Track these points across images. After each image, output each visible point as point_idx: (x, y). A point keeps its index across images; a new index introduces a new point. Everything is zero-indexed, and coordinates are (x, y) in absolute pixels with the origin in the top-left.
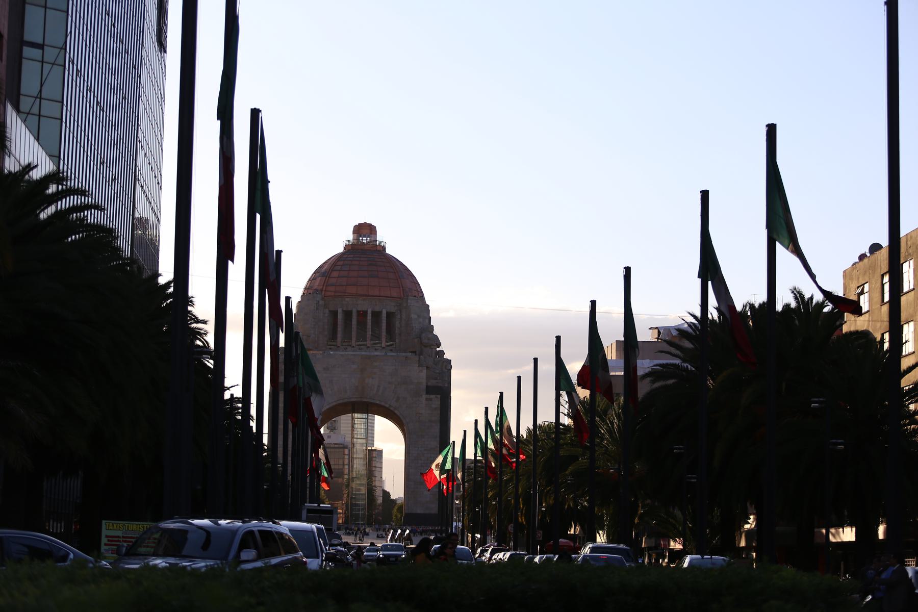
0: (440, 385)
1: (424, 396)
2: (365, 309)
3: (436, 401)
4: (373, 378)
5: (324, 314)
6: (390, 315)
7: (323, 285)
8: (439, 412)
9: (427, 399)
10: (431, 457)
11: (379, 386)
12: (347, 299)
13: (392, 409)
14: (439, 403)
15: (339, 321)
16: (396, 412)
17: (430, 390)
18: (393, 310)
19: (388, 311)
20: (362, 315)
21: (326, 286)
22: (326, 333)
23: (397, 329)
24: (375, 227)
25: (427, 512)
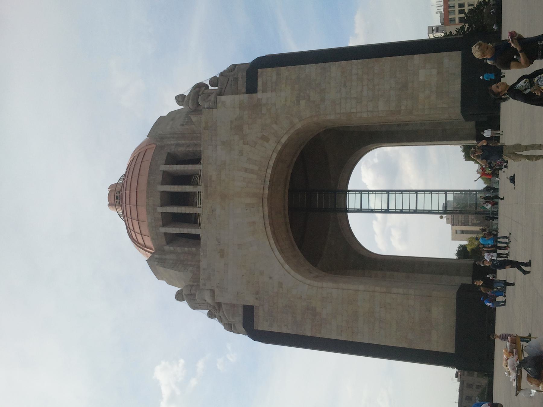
0: (245, 74)
1: (259, 95)
2: (159, 195)
5: (171, 252)
6: (172, 159)
7: (146, 251)
9: (264, 91)
11: (246, 170)
13: (279, 147)
14: (269, 70)
15: (175, 232)
16: (284, 140)
17: (252, 89)
18: (164, 156)
19: (164, 162)
21: (146, 247)
22: (194, 249)
23: (187, 149)
24: (111, 187)
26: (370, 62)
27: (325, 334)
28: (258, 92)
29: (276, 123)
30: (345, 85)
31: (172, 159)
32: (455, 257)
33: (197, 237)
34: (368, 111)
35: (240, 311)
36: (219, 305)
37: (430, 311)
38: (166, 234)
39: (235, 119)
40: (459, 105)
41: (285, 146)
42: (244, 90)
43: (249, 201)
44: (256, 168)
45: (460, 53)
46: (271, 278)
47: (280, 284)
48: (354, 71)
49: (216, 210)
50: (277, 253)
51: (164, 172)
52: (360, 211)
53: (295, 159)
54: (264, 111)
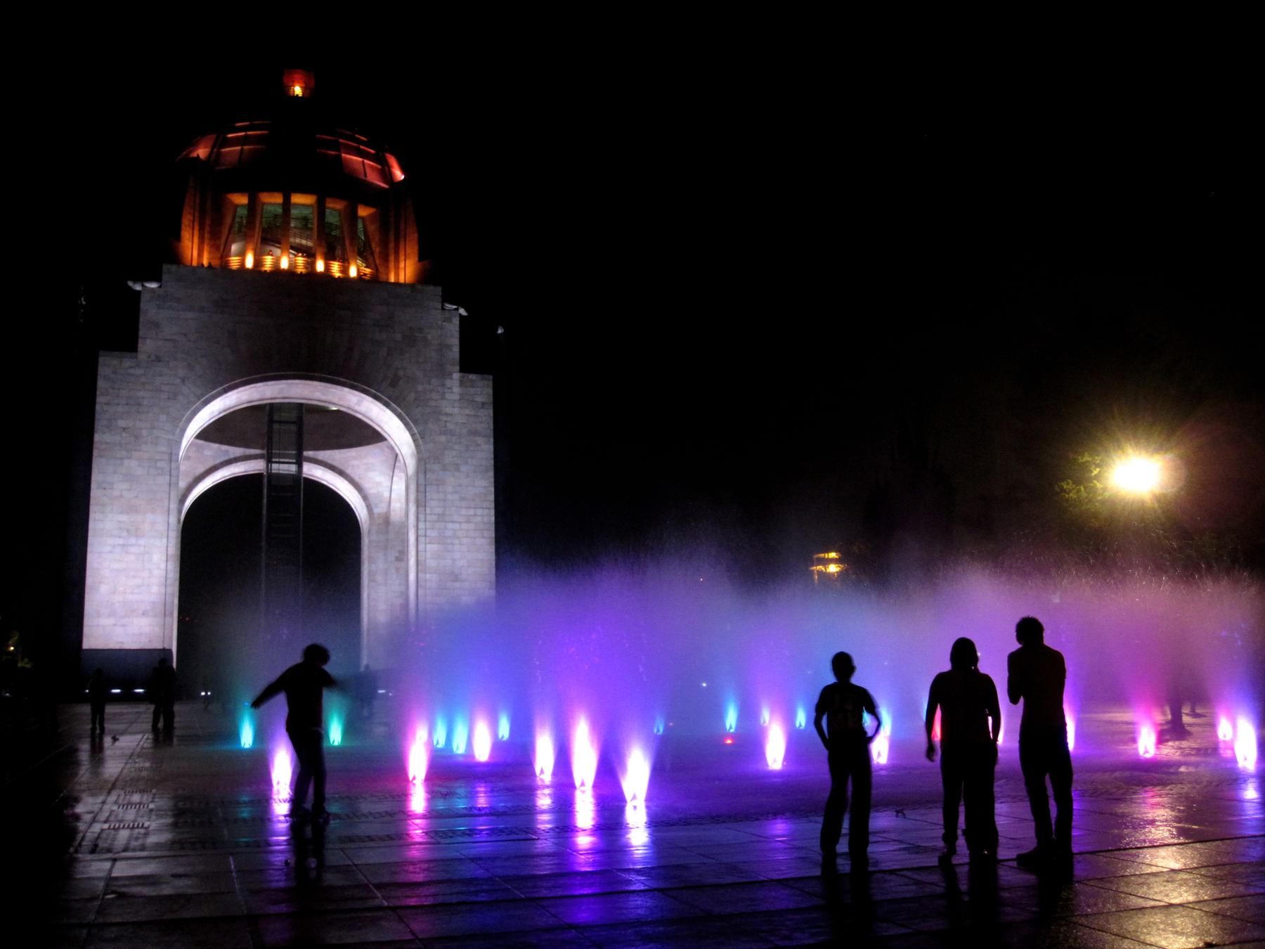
1: (456, 376)
8: (491, 412)
9: (462, 384)
10: (475, 515)
14: (490, 391)
28: (461, 374)
29: (415, 399)
30: (462, 499)
34: (426, 529)
37: (143, 614)
48: (479, 512)
54: (433, 381)
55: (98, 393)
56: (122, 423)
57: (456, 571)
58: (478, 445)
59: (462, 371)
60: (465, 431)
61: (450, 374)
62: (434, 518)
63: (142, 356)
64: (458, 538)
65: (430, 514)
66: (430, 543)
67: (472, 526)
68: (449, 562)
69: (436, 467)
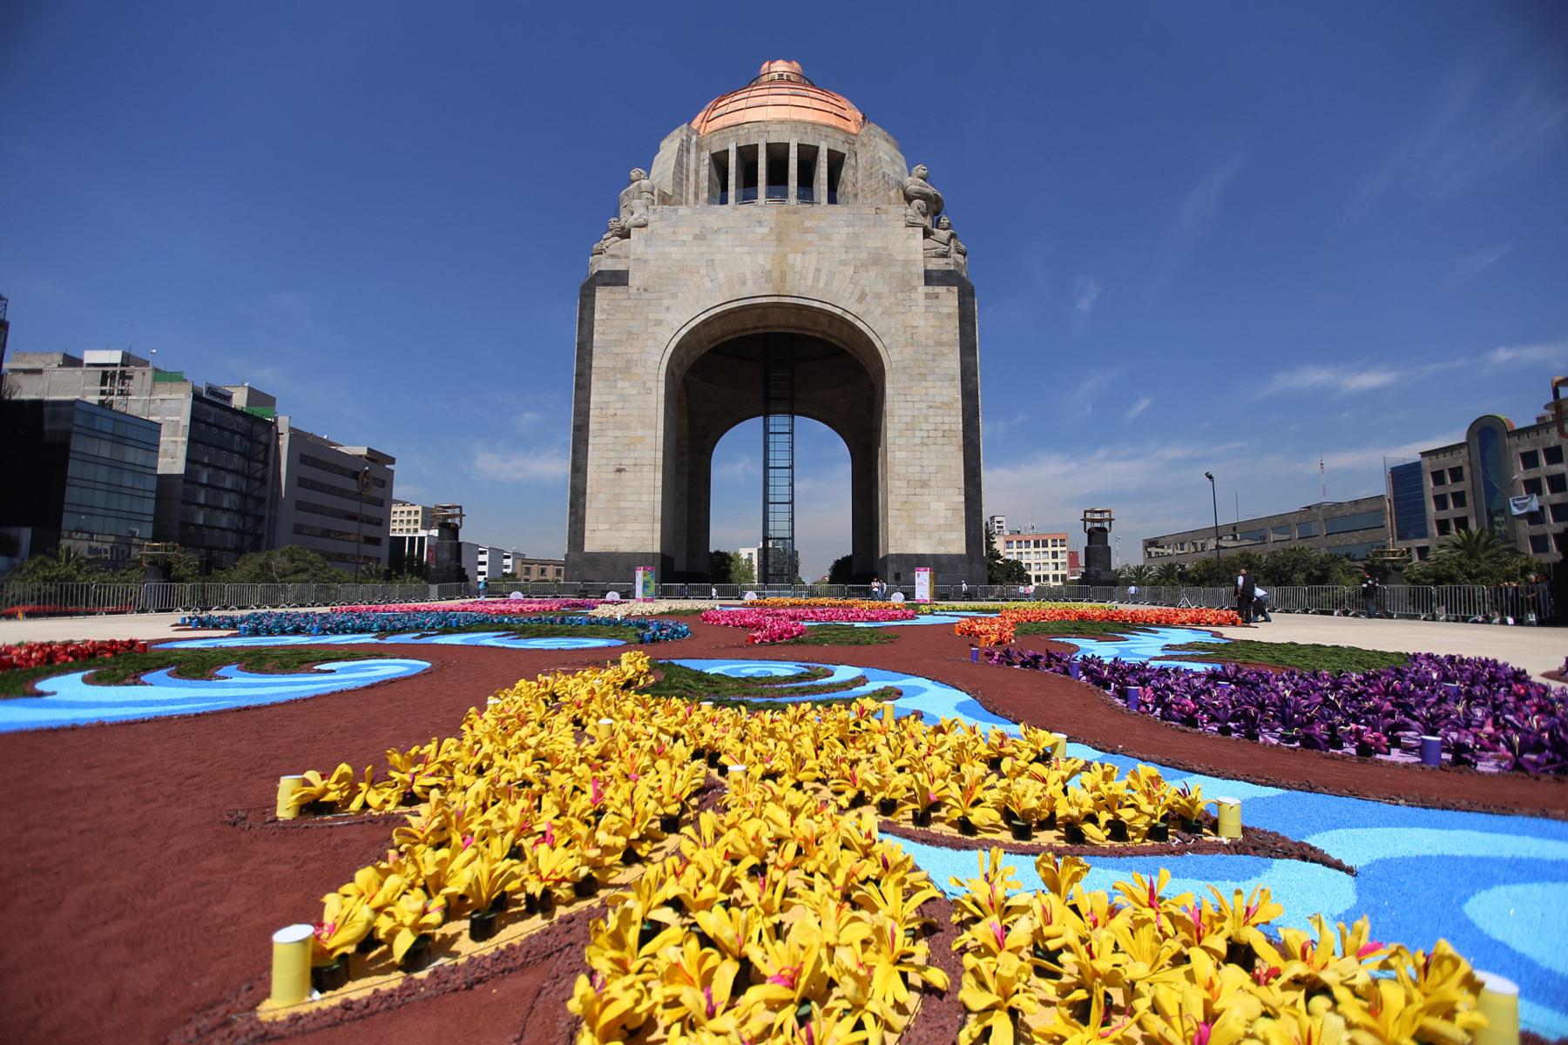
0: (952, 268)
1: (922, 289)
3: (949, 299)
4: (803, 253)
9: (927, 296)
11: (818, 270)
12: (746, 126)
13: (849, 317)
14: (956, 303)
15: (730, 166)
16: (859, 324)
17: (930, 278)
18: (839, 149)
19: (832, 148)
20: (778, 156)
23: (849, 184)
25: (941, 550)
26: (959, 439)
27: (596, 386)
29: (883, 313)
30: (930, 407)
31: (836, 161)
32: (712, 550)
33: (724, 201)
35: (620, 267)
36: (628, 236)
38: (727, 151)
39: (890, 255)
40: (899, 551)
41: (851, 326)
42: (929, 267)
43: (776, 274)
44: (821, 285)
45: (964, 551)
46: (668, 309)
47: (659, 323)
48: (947, 419)
49: (761, 226)
50: (703, 317)
51: (817, 148)
52: (767, 433)
53: (833, 341)
54: (899, 295)
55: (595, 324)
56: (614, 350)
57: (925, 477)
58: (943, 355)
59: (927, 283)
60: (931, 342)
61: (915, 288)
62: (902, 426)
63: (633, 290)
64: (927, 445)
65: (899, 422)
66: (899, 450)
67: (941, 434)
68: (918, 469)
69: (904, 377)
